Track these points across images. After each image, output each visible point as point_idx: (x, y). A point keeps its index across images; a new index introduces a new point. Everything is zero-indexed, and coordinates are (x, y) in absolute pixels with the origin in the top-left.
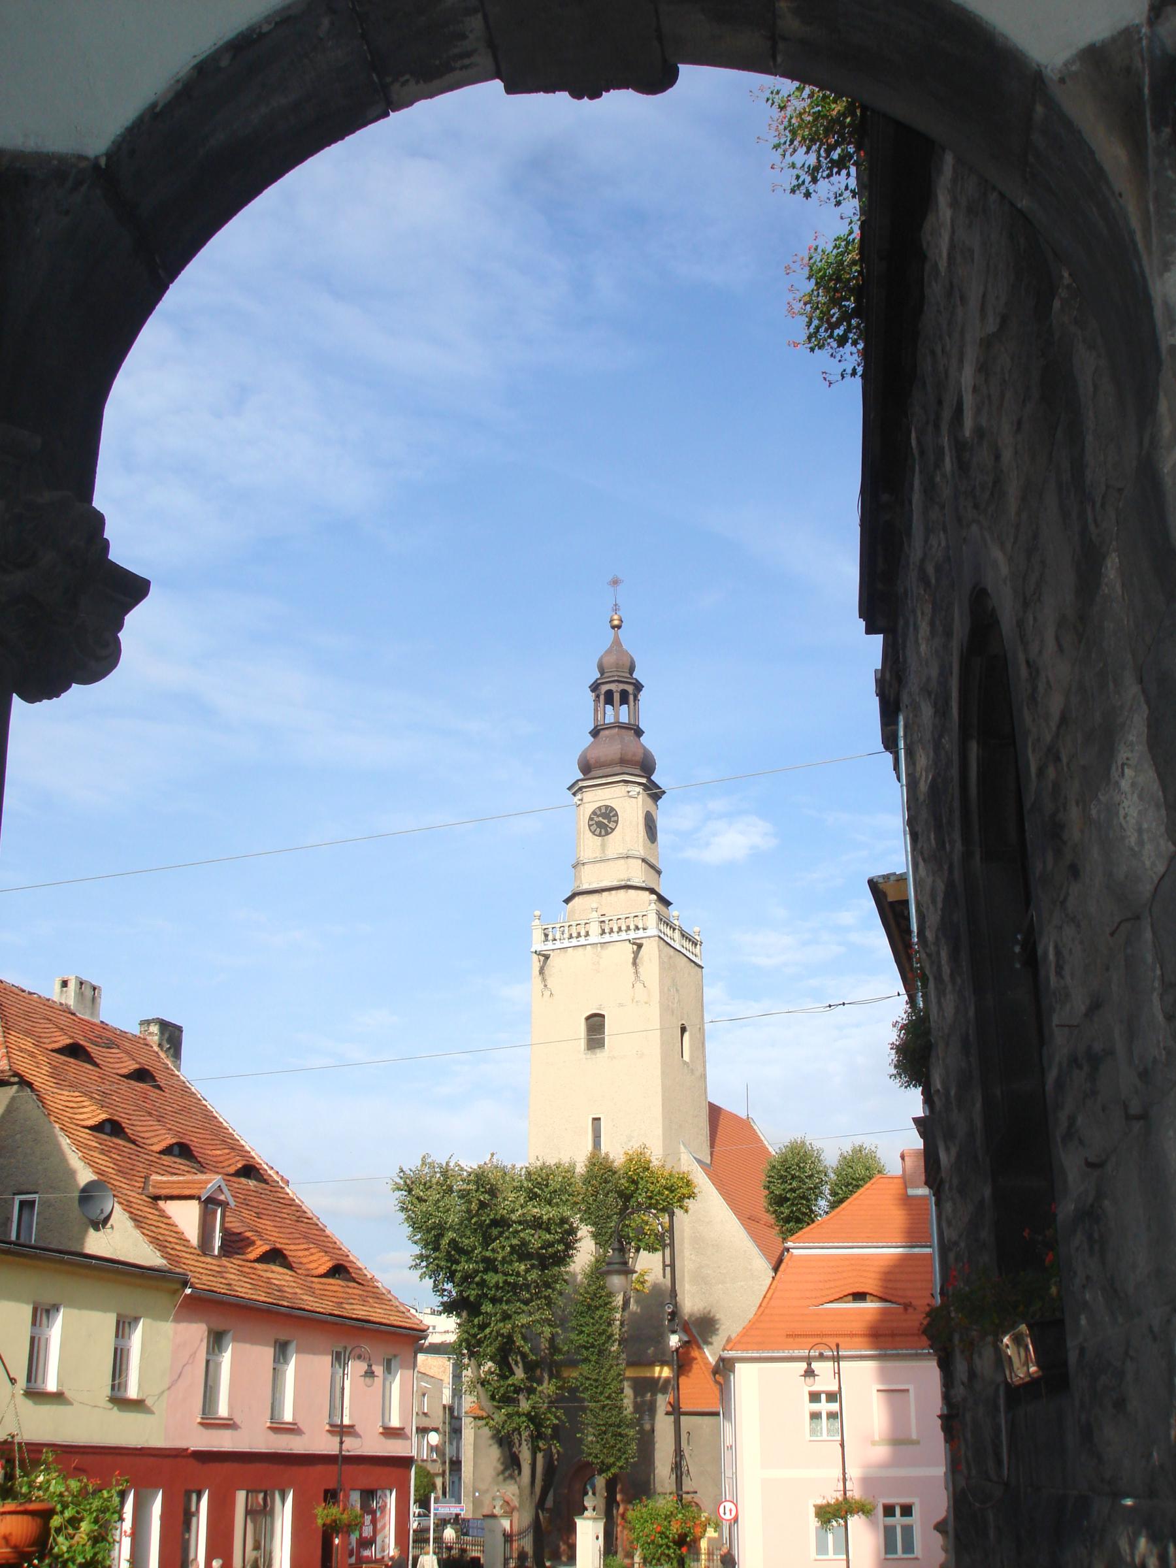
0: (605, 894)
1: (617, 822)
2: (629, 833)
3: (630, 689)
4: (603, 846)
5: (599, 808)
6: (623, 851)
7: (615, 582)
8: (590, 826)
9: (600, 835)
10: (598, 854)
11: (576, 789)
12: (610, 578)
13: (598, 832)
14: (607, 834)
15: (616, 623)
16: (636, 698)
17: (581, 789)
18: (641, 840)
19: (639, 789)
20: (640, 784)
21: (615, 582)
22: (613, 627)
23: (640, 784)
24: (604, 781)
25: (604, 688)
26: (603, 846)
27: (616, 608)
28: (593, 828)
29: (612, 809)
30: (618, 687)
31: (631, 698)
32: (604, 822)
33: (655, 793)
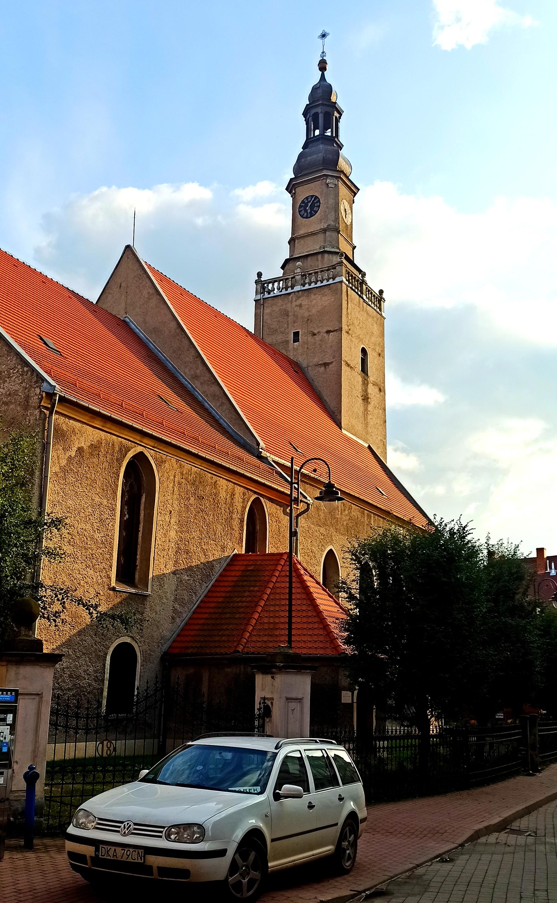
7: (324, 36)
12: (319, 33)
16: (337, 121)
21: (324, 36)
25: (313, 111)
29: (316, 197)
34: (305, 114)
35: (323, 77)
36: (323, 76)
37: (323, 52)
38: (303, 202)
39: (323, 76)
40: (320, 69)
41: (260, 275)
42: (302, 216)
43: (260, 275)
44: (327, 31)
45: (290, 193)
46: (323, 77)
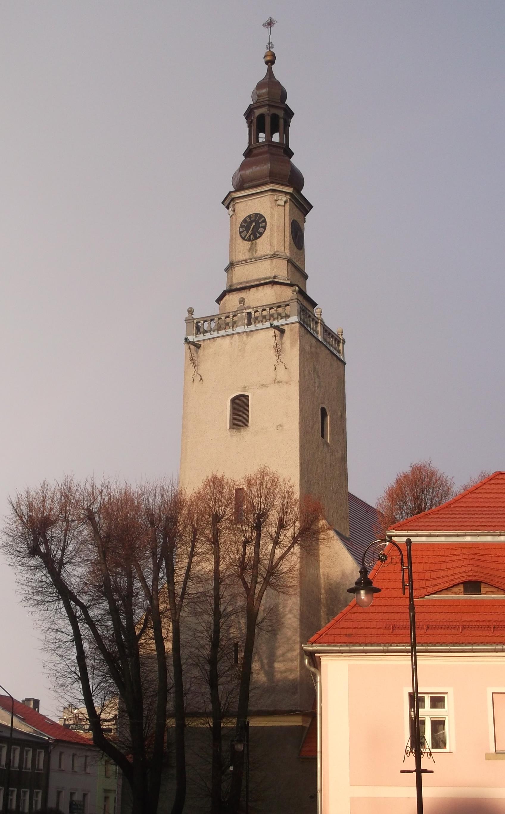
0: (253, 290)
2: (275, 237)
3: (281, 113)
6: (269, 252)
7: (270, 24)
8: (241, 232)
9: (249, 240)
10: (247, 256)
11: (229, 202)
12: (265, 20)
14: (256, 238)
17: (233, 199)
18: (287, 243)
20: (286, 193)
21: (270, 24)
23: (286, 193)
24: (254, 191)
25: (258, 112)
26: (252, 249)
28: (243, 235)
29: (261, 216)
30: (270, 113)
31: (281, 122)
32: (253, 228)
33: (302, 206)
34: (249, 114)
35: (270, 72)
37: (270, 43)
38: (245, 221)
40: (267, 63)
41: (191, 311)
42: (244, 239)
43: (191, 311)
44: (274, 18)
45: (228, 207)
46: (270, 72)
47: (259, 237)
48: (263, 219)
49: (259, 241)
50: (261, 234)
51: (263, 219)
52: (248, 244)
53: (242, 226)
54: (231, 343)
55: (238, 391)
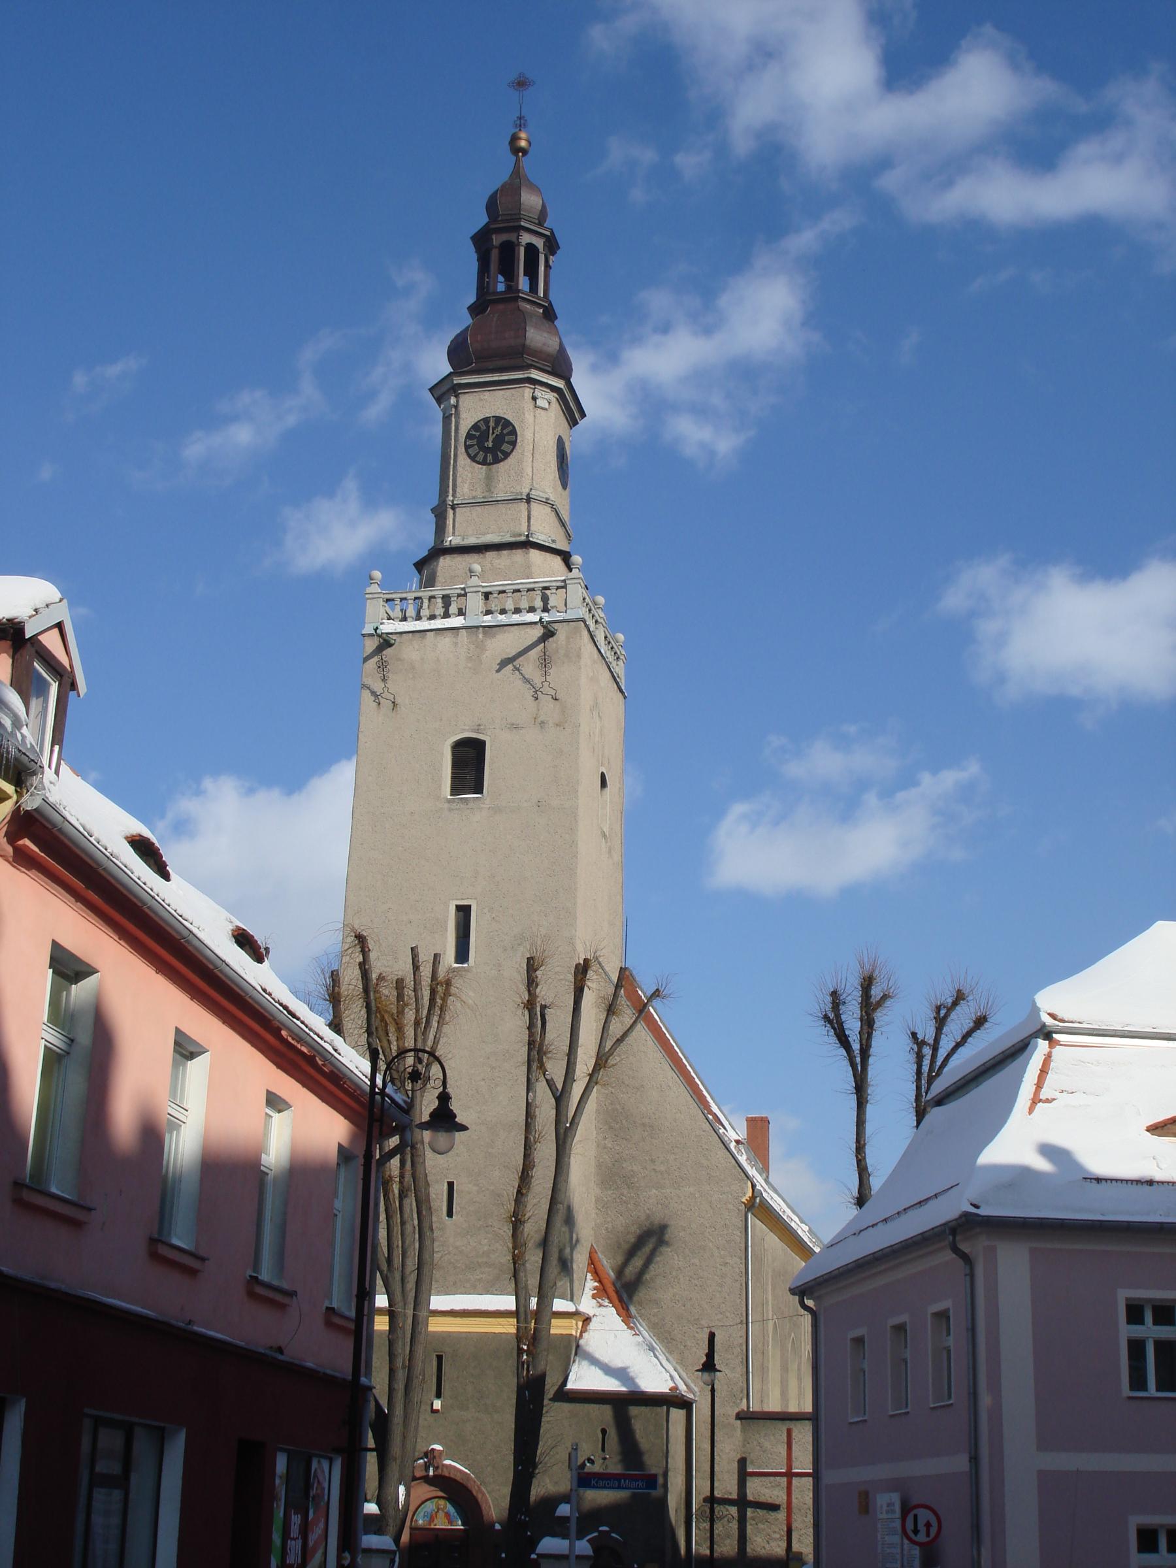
0: (490, 555)
1: (514, 444)
3: (539, 243)
4: (489, 481)
5: (486, 420)
7: (521, 84)
8: (467, 447)
9: (484, 463)
13: (481, 457)
14: (497, 461)
15: (523, 144)
19: (552, 396)
20: (553, 389)
21: (521, 84)
22: (516, 150)
23: (553, 389)
27: (521, 123)
28: (472, 451)
29: (507, 423)
36: (517, 162)
37: (520, 118)
38: (475, 427)
39: (517, 162)
42: (473, 458)
47: (502, 460)
48: (511, 428)
49: (502, 466)
50: (507, 455)
51: (511, 428)
52: (481, 470)
53: (469, 436)
54: (456, 644)
55: (463, 730)
